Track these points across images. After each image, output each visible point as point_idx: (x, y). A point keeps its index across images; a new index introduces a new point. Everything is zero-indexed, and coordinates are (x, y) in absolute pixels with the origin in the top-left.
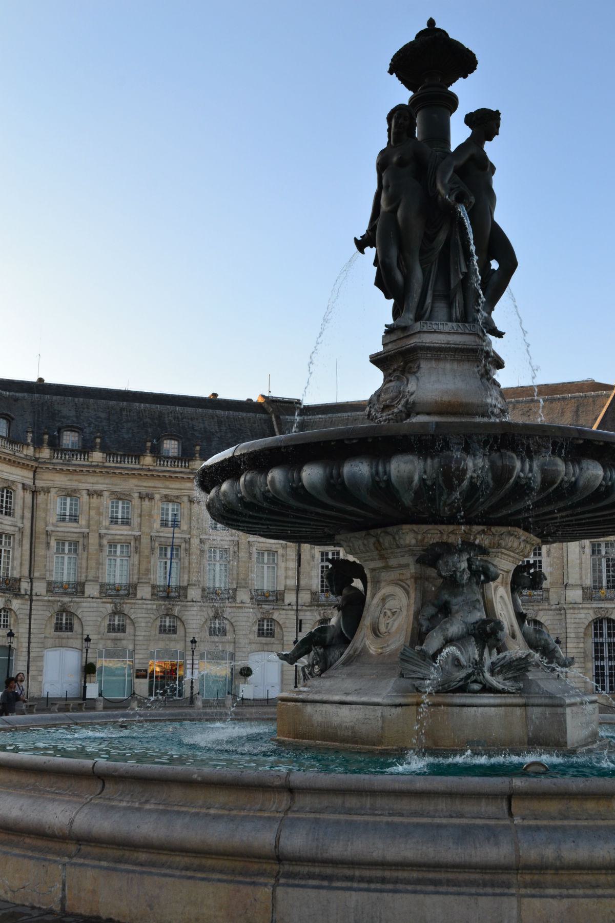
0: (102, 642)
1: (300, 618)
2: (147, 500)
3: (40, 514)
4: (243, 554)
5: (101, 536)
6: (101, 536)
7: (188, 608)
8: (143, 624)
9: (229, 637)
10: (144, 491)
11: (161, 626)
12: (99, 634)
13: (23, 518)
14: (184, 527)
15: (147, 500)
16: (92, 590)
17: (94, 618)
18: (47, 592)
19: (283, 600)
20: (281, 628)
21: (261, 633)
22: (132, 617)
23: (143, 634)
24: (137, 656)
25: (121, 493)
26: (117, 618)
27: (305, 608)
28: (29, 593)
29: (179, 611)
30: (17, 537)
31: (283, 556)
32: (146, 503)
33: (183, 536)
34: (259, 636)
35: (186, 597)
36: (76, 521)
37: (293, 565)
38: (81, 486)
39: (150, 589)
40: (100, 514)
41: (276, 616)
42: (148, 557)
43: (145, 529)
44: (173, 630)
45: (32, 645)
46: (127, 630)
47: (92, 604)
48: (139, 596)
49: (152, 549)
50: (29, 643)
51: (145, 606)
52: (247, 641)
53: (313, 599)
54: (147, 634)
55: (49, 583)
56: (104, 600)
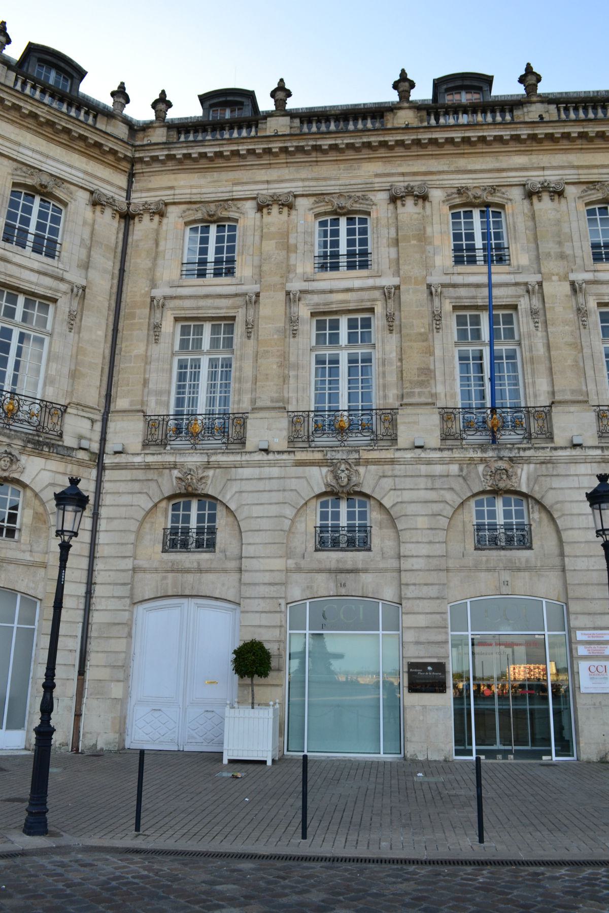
0: (295, 577)
2: (410, 201)
3: (138, 262)
5: (291, 298)
6: (291, 298)
7: (562, 469)
8: (422, 522)
10: (401, 184)
11: (479, 528)
12: (289, 555)
13: (86, 266)
14: (520, 255)
15: (410, 201)
16: (268, 431)
17: (274, 510)
18: (146, 445)
22: (387, 503)
23: (424, 550)
24: (407, 621)
25: (341, 195)
26: (343, 508)
28: (95, 447)
29: (535, 479)
30: (64, 304)
32: (410, 208)
33: (521, 278)
36: (230, 272)
38: (240, 191)
39: (436, 419)
40: (289, 249)
42: (424, 338)
43: (411, 269)
44: (520, 539)
45: (98, 591)
46: (376, 541)
47: (267, 471)
48: (402, 441)
49: (437, 317)
50: (90, 584)
51: (424, 469)
54: (439, 550)
55: (152, 424)
56: (300, 456)
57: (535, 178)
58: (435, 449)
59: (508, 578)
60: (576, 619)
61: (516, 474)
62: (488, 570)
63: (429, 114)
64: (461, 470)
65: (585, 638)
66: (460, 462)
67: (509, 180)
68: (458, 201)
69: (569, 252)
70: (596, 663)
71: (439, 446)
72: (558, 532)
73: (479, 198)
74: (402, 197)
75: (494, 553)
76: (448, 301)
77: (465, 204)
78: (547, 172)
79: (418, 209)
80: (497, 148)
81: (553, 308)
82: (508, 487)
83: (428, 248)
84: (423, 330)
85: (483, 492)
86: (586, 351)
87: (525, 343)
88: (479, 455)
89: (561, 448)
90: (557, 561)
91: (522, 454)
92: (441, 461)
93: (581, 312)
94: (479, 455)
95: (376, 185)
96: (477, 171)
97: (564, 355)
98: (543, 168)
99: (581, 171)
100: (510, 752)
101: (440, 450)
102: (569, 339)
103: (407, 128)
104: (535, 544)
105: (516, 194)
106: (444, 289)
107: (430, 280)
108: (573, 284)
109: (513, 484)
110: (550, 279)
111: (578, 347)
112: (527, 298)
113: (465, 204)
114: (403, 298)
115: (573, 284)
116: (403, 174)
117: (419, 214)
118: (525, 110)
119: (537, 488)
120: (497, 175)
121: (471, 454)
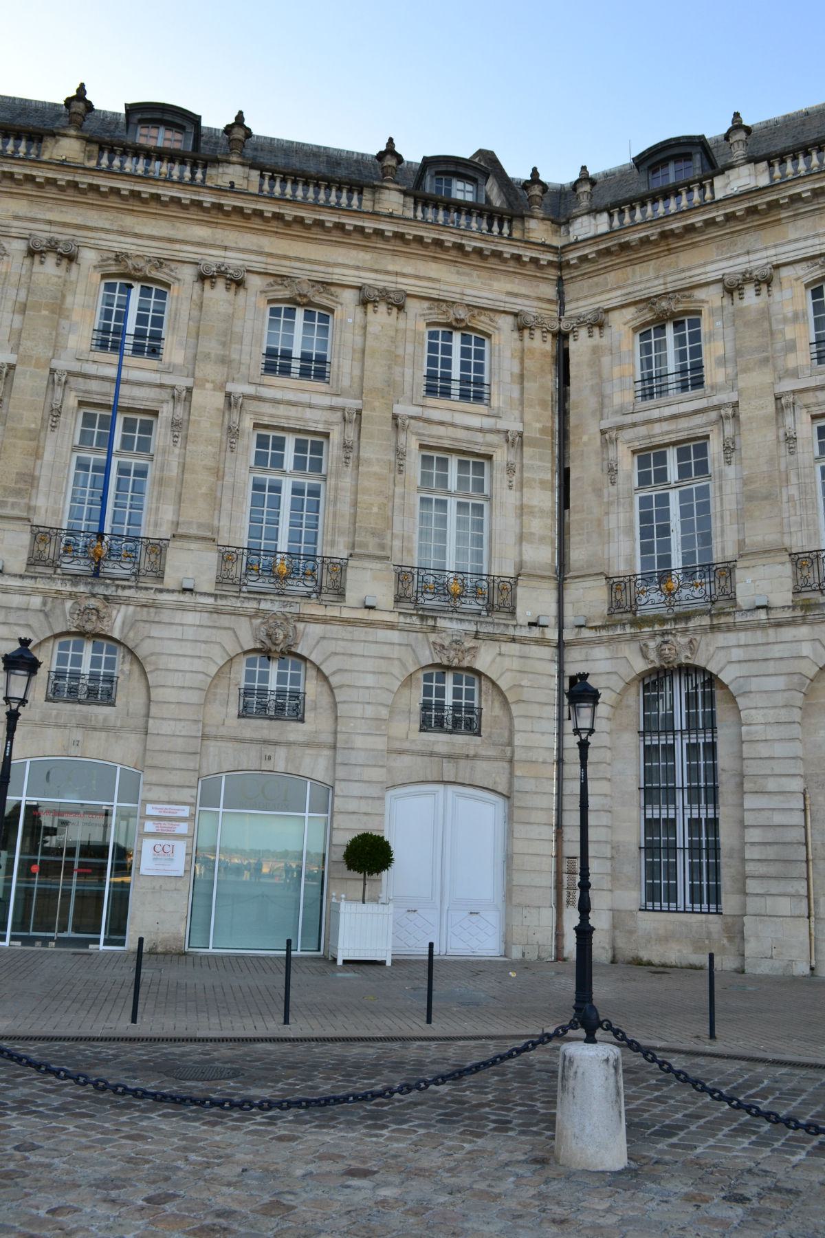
2: (51, 260)
4: (375, 451)
7: (165, 616)
9: (316, 722)
10: (43, 234)
14: (174, 350)
15: (51, 260)
19: (513, 613)
20: (505, 703)
21: (432, 719)
27: (586, 633)
29: (130, 624)
32: (50, 268)
33: (167, 380)
34: (425, 726)
35: (160, 577)
37: (547, 500)
39: (26, 538)
41: (485, 660)
42: (35, 435)
52: (380, 743)
53: (615, 607)
57: (213, 258)
58: (15, 575)
59: (79, 737)
60: (149, 790)
61: (110, 616)
62: (58, 726)
63: (101, 150)
64: (44, 604)
65: (156, 813)
66: (45, 594)
67: (181, 254)
68: (114, 269)
69: (235, 356)
70: (163, 842)
71: (22, 572)
72: (148, 688)
73: (140, 270)
74: (42, 252)
75: (69, 707)
76: (73, 394)
77: (123, 275)
78: (229, 254)
79: (60, 271)
80: (174, 211)
81: (199, 422)
82: (97, 630)
83: (64, 323)
84: (33, 426)
85: (68, 633)
86: (228, 479)
87: (158, 458)
88: (68, 588)
89: (168, 591)
90: (140, 722)
91: (120, 592)
92: (21, 591)
93: (233, 433)
94: (68, 588)
95: (13, 230)
96: (143, 235)
97: (201, 481)
98: (226, 248)
99: (270, 260)
100: (52, 939)
101: (22, 577)
102: (210, 462)
103: (63, 165)
104: (120, 700)
105: (188, 273)
106: (71, 379)
107: (55, 364)
108: (228, 395)
109: (103, 627)
110: (202, 387)
111: (218, 473)
112: (171, 404)
113: (123, 275)
114: (16, 381)
115: (228, 395)
116: (50, 222)
117: (60, 277)
118: (220, 170)
119: (131, 635)
120: (168, 245)
121: (58, 586)
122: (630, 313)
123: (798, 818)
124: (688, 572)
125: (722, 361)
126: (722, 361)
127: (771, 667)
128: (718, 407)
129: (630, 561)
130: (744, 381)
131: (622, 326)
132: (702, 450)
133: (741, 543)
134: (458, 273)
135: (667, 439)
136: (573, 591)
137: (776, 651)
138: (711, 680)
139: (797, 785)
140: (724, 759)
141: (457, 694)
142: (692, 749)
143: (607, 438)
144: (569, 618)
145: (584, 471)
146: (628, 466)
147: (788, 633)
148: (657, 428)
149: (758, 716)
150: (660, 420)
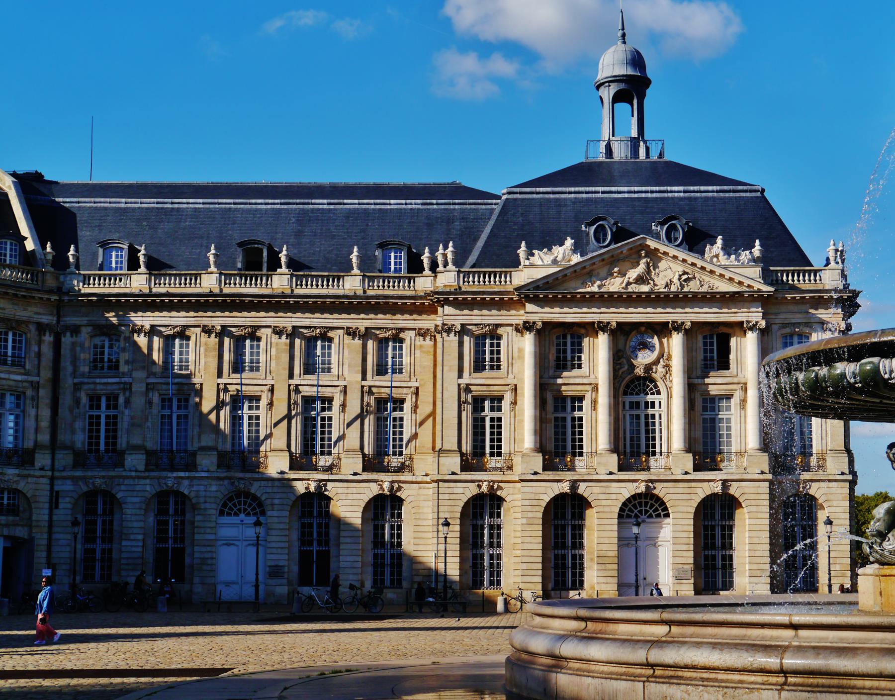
1: (56, 488)
19: (32, 463)
31: (33, 399)
41: (21, 486)
122: (89, 329)
123: (140, 549)
124: (107, 451)
125: (127, 362)
126: (127, 362)
127: (135, 494)
128: (125, 383)
129: (83, 443)
130: (136, 374)
131: (85, 332)
132: (116, 398)
133: (128, 442)
134: (13, 304)
135: (102, 392)
136: (60, 455)
137: (138, 488)
138: (113, 496)
139: (140, 537)
140: (116, 527)
141: (9, 499)
142: (104, 522)
143: (77, 387)
144: (56, 467)
145: (66, 400)
146: (84, 400)
147: (142, 482)
148: (98, 387)
149: (129, 512)
150: (100, 384)
